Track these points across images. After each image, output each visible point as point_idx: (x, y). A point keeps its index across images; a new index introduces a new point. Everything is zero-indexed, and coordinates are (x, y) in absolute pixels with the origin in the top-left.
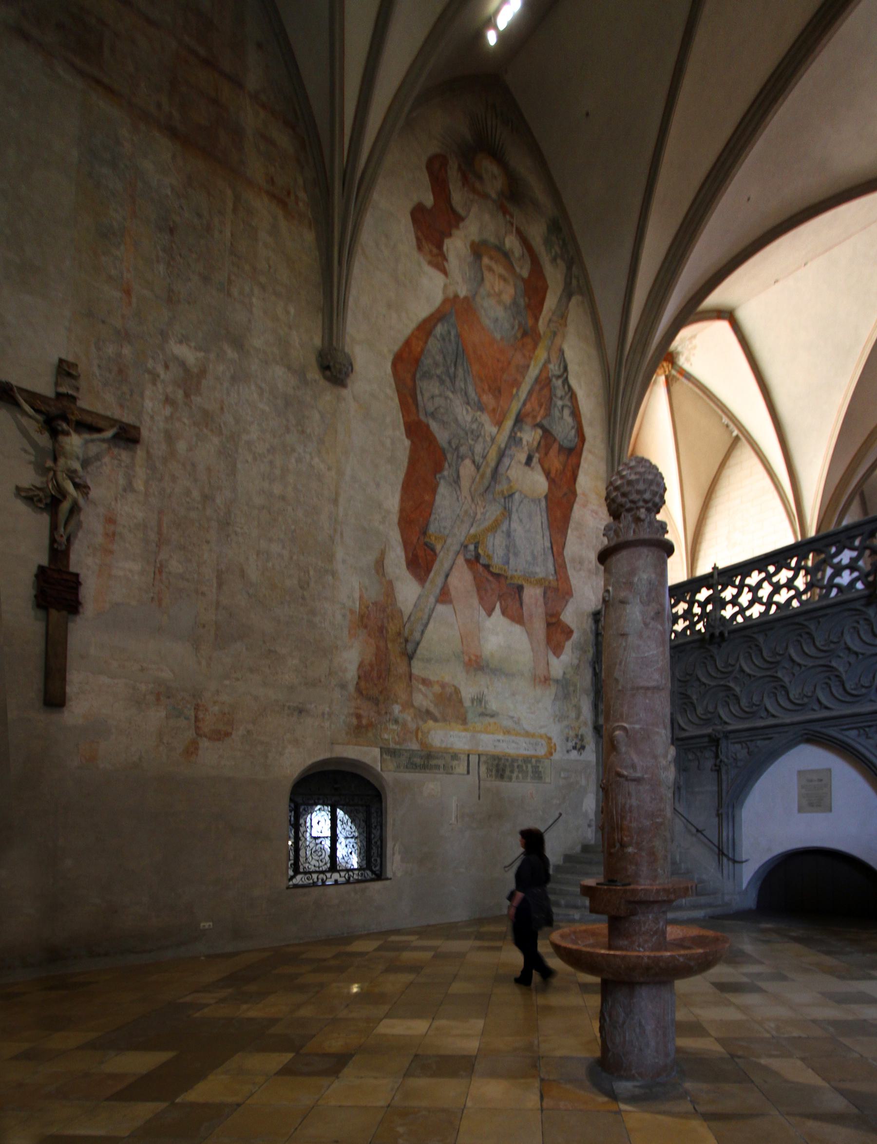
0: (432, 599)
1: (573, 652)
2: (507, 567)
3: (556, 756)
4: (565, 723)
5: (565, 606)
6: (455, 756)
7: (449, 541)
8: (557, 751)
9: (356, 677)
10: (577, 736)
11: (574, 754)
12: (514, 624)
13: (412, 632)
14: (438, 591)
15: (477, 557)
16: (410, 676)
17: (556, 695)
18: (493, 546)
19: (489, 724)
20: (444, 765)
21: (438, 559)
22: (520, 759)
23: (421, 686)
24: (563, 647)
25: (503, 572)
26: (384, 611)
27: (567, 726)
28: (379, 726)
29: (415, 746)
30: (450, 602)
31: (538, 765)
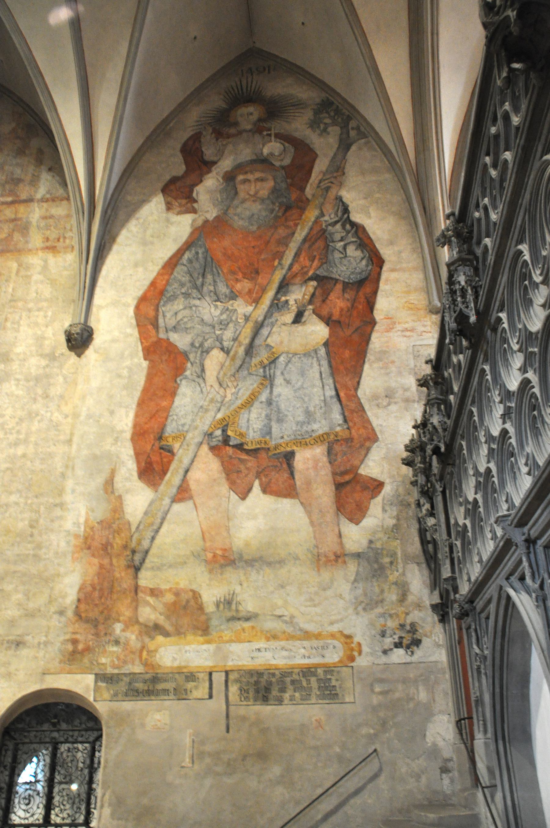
0: (167, 501)
1: (384, 510)
2: (268, 437)
3: (362, 662)
4: (379, 610)
5: (366, 455)
6: (191, 677)
7: (190, 435)
8: (364, 653)
9: (76, 602)
10: (402, 626)
11: (399, 655)
12: (280, 499)
13: (139, 543)
14: (174, 490)
15: (226, 440)
16: (136, 589)
17: (357, 573)
18: (248, 420)
19: (243, 630)
20: (175, 689)
21: (176, 458)
22: (296, 671)
23: (149, 598)
24: (367, 508)
25: (263, 446)
27: (383, 615)
28: (97, 650)
29: (138, 669)
30: (191, 498)
31: (329, 677)
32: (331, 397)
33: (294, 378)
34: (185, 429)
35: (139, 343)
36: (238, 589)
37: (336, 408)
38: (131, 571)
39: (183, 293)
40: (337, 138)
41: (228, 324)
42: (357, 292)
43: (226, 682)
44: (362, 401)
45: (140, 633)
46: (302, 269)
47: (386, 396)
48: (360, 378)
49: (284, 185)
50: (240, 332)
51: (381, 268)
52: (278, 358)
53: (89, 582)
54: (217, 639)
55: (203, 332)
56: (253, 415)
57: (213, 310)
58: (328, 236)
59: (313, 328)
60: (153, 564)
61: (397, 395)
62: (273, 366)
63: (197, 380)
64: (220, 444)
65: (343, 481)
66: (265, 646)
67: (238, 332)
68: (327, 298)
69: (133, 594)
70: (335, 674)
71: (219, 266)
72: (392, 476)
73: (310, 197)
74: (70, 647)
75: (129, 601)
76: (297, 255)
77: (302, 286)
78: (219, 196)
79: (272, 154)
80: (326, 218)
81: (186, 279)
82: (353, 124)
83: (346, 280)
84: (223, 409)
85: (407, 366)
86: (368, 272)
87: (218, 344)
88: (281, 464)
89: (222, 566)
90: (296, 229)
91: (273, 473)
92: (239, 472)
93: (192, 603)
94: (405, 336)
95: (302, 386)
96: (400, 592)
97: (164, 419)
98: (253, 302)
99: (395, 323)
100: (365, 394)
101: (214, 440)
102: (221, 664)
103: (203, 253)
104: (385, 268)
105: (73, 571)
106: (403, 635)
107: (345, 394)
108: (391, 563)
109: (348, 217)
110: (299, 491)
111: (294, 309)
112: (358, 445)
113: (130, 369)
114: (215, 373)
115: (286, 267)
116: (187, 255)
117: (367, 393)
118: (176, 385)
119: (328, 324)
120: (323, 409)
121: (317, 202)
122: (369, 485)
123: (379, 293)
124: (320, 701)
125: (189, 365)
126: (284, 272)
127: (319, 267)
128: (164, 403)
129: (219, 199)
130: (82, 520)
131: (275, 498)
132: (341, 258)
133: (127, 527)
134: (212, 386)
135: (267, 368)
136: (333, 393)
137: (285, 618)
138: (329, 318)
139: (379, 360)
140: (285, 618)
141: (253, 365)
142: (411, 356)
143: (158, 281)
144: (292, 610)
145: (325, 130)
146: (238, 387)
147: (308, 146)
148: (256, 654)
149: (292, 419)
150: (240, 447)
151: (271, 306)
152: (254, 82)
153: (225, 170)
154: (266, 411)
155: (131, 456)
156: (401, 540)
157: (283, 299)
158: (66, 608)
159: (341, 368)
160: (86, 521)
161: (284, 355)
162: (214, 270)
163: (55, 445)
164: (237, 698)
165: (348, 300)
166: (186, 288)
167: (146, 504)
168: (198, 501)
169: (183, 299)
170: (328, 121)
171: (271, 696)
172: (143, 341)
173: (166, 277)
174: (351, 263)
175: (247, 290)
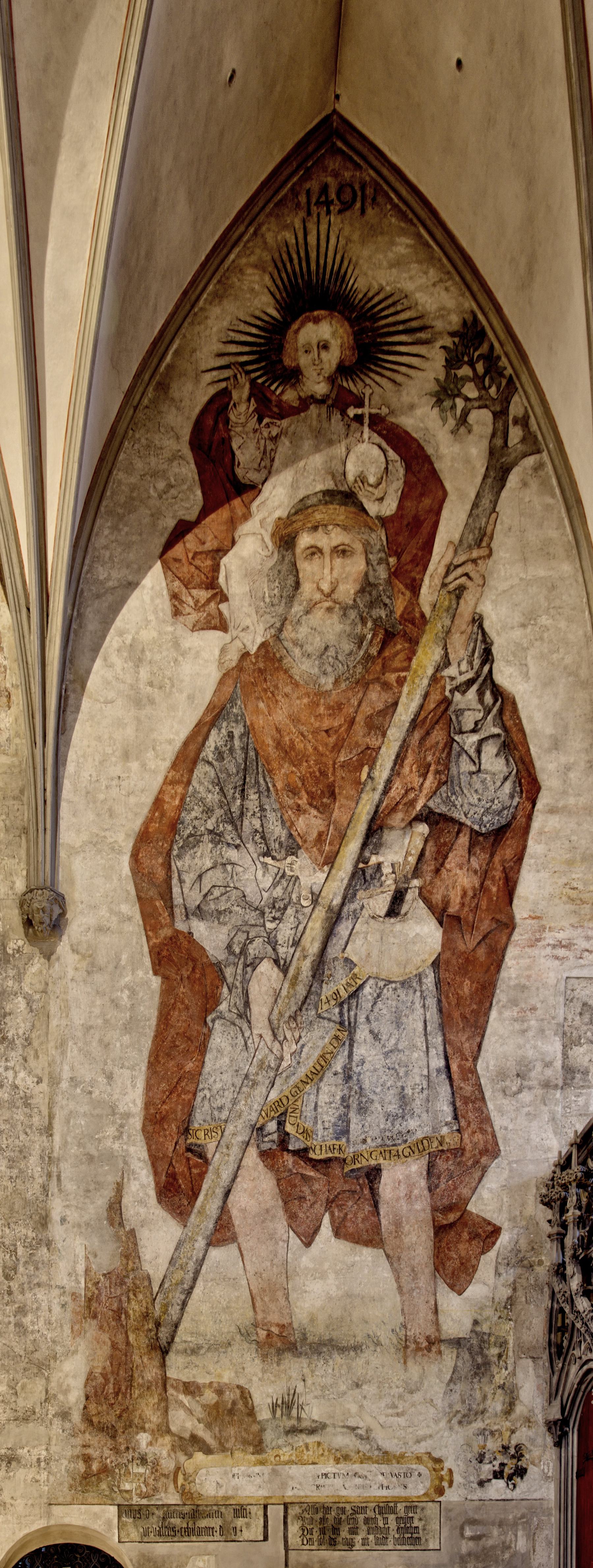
0: (201, 1243)
2: (344, 1140)
3: (452, 1496)
4: (479, 1425)
6: (241, 1511)
7: (230, 1128)
8: (455, 1484)
9: (83, 1399)
10: (505, 1448)
15: (284, 1140)
16: (165, 1380)
21: (211, 1168)
22: (373, 1505)
23: (182, 1397)
24: (475, 1269)
25: (337, 1155)
26: (122, 1283)
27: (482, 1432)
28: (117, 1471)
29: (172, 1498)
30: (234, 1239)
31: (410, 1515)
32: (438, 1071)
33: (385, 1028)
34: (224, 1115)
35: (144, 939)
36: (300, 1389)
37: (444, 1090)
38: (157, 1355)
39: (211, 832)
40: (485, 444)
41: (285, 908)
42: (492, 855)
43: (285, 1517)
44: (483, 1081)
45: (173, 1448)
46: (407, 792)
47: (518, 1075)
48: (483, 1036)
49: (382, 573)
50: (305, 928)
51: (534, 804)
52: (361, 987)
53: (99, 1370)
54: (272, 1459)
55: (246, 923)
56: (323, 1098)
57: (260, 873)
58: (454, 718)
59: (418, 929)
60: (184, 1345)
61: (533, 1074)
62: (354, 1002)
63: (237, 1021)
64: (275, 1147)
65: (445, 1222)
66: (334, 1470)
67: (301, 927)
68: (442, 865)
69: (160, 1390)
70: (418, 1511)
71: (270, 771)
72: (512, 1219)
73: (427, 610)
74: (81, 1467)
75: (156, 1400)
76: (399, 759)
77: (405, 834)
78: (266, 590)
79: (362, 479)
80: (452, 671)
81: (213, 798)
83: (476, 827)
84: (278, 1081)
85: (553, 1018)
86: (512, 810)
87: (269, 948)
88: (362, 1189)
89: (280, 1352)
90: (400, 692)
91: (350, 1203)
92: (302, 1199)
93: (240, 1405)
94: (557, 958)
95: (396, 1044)
96: (507, 1400)
97: (190, 1096)
98: (325, 863)
99: (543, 929)
100: (488, 1067)
101: (266, 1139)
102: (279, 1493)
103: (241, 736)
104: (539, 806)
105: (75, 1352)
106: (505, 1461)
107: (459, 1066)
108: (500, 1356)
109: (490, 671)
110: (385, 1235)
112: (470, 1163)
113: (133, 993)
114: (265, 1011)
115: (381, 787)
116: (215, 739)
117: (491, 1068)
118: (205, 1030)
119: (441, 923)
120: (426, 1092)
121: (439, 626)
122: (480, 1230)
123: (526, 861)
124: (399, 1547)
125: (225, 990)
126: (377, 796)
127: (435, 793)
128: (190, 1066)
129: (267, 600)
130: (81, 1268)
131: (352, 1245)
132: (471, 773)
133: (146, 1283)
134: (261, 1036)
135: (346, 1006)
136: (442, 1063)
137: (359, 1431)
138: (444, 910)
139: (514, 1002)
140: (359, 1431)
141: (323, 997)
142: (561, 999)
143: (167, 798)
144: (369, 1419)
145: (463, 420)
146: (301, 1042)
147: (427, 459)
148: (321, 1481)
149: (380, 1108)
150: (302, 1154)
151: (353, 875)
152: (333, 241)
153: (278, 514)
154: (342, 1090)
155: (144, 1161)
156: (516, 1322)
157: (374, 860)
158: (70, 1408)
159: (456, 1014)
160: (87, 1271)
161: (371, 982)
162: (262, 781)
163: (26, 1133)
164: (299, 1540)
165: (476, 872)
166: (213, 820)
167: (172, 1247)
168: (244, 1246)
169: (210, 845)
170: (471, 391)
171: (340, 1539)
172: (150, 933)
173: (180, 789)
174: (486, 788)
175: (315, 835)
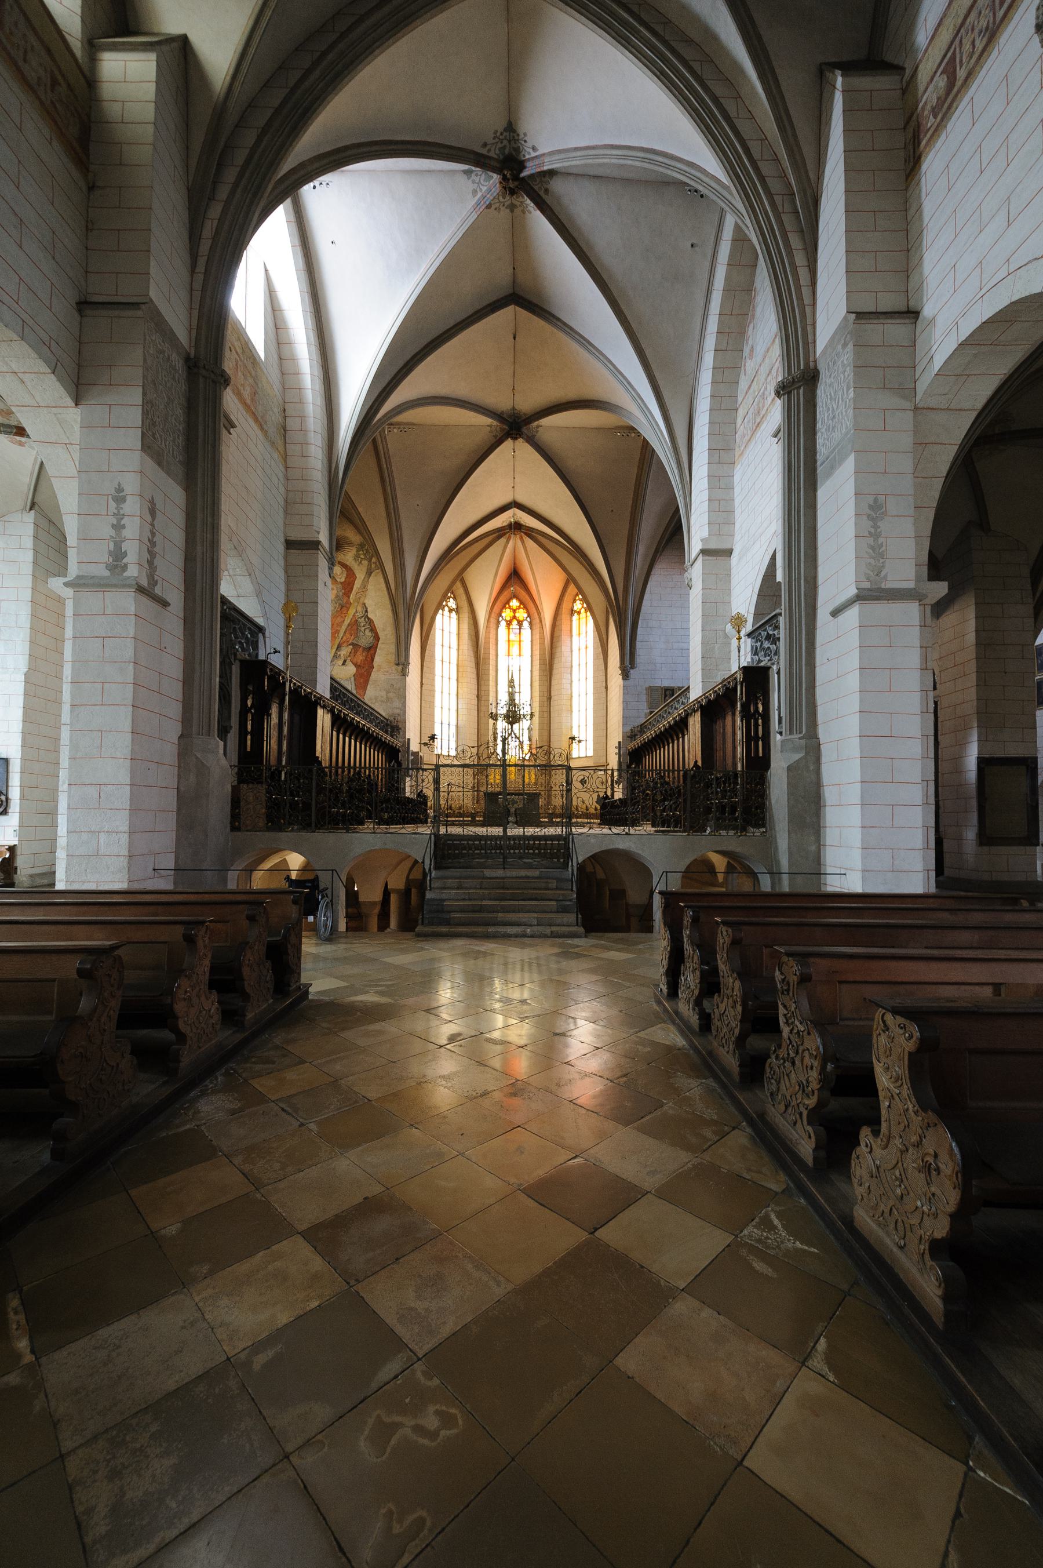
49: (341, 594)
73: (352, 601)
76: (345, 632)
80: (358, 614)
82: (374, 560)
111: (343, 659)
145: (361, 562)
170: (362, 556)
